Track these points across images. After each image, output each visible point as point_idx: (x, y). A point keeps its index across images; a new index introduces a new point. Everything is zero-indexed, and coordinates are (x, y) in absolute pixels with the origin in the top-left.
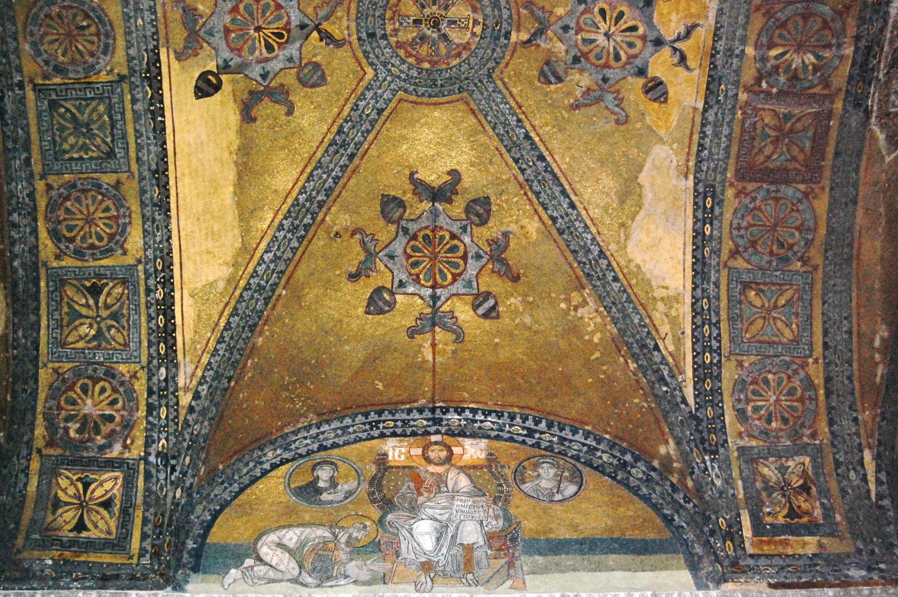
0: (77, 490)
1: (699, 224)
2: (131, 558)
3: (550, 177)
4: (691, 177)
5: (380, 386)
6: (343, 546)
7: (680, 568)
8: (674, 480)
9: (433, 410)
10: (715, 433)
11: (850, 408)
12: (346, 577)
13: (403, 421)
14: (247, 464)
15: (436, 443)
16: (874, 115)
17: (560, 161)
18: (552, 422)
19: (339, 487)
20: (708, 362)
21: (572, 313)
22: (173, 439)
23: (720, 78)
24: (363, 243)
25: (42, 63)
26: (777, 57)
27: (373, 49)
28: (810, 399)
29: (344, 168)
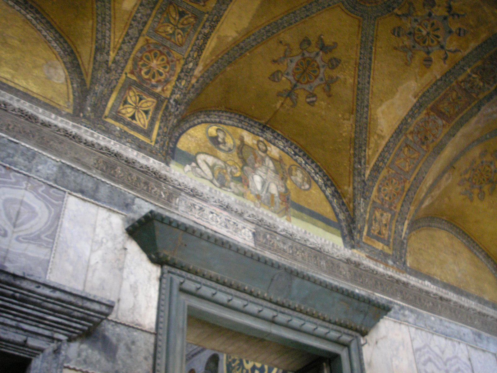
0: (136, 100)
2: (151, 142)
4: (417, 99)
8: (344, 201)
9: (264, 127)
12: (230, 188)
15: (261, 141)
19: (226, 145)
22: (182, 96)
24: (286, 51)
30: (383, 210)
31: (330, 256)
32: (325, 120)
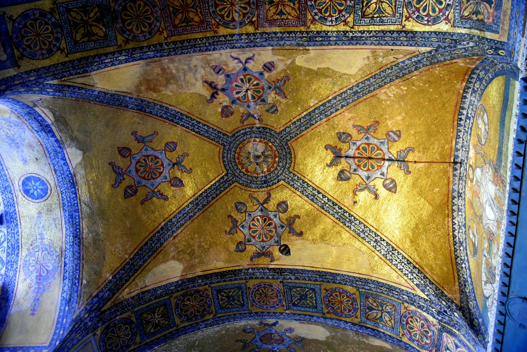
1: (331, 43)
4: (307, 48)
5: (437, 190)
9: (455, 163)
10: (446, 39)
13: (460, 179)
14: (462, 268)
18: (460, 107)
21: (392, 98)
22: (433, 305)
24: (361, 190)
25: (278, 306)
27: (272, 181)
29: (324, 196)
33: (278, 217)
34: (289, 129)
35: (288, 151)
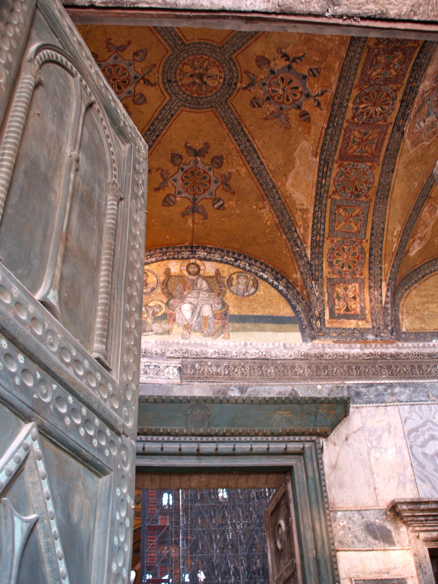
1: (320, 179)
3: (252, 149)
4: (318, 157)
5: (168, 237)
6: (151, 316)
7: (296, 331)
8: (298, 290)
9: (192, 247)
11: (379, 262)
12: (152, 331)
15: (193, 264)
16: (406, 134)
17: (257, 144)
19: (149, 286)
20: (318, 240)
21: (258, 211)
23: (336, 116)
24: (162, 175)
26: (363, 108)
27: (170, 87)
28: (362, 258)
30: (345, 283)
31: (280, 360)
32: (243, 217)
33: (128, 95)
34: (230, 113)
35: (204, 107)
